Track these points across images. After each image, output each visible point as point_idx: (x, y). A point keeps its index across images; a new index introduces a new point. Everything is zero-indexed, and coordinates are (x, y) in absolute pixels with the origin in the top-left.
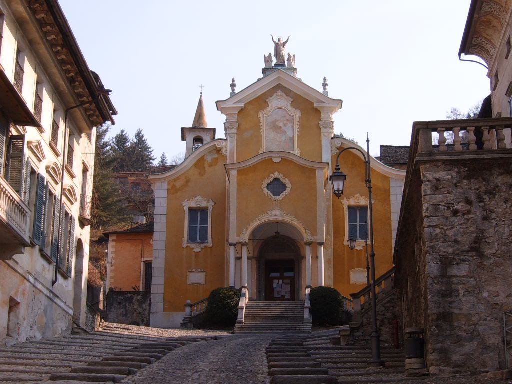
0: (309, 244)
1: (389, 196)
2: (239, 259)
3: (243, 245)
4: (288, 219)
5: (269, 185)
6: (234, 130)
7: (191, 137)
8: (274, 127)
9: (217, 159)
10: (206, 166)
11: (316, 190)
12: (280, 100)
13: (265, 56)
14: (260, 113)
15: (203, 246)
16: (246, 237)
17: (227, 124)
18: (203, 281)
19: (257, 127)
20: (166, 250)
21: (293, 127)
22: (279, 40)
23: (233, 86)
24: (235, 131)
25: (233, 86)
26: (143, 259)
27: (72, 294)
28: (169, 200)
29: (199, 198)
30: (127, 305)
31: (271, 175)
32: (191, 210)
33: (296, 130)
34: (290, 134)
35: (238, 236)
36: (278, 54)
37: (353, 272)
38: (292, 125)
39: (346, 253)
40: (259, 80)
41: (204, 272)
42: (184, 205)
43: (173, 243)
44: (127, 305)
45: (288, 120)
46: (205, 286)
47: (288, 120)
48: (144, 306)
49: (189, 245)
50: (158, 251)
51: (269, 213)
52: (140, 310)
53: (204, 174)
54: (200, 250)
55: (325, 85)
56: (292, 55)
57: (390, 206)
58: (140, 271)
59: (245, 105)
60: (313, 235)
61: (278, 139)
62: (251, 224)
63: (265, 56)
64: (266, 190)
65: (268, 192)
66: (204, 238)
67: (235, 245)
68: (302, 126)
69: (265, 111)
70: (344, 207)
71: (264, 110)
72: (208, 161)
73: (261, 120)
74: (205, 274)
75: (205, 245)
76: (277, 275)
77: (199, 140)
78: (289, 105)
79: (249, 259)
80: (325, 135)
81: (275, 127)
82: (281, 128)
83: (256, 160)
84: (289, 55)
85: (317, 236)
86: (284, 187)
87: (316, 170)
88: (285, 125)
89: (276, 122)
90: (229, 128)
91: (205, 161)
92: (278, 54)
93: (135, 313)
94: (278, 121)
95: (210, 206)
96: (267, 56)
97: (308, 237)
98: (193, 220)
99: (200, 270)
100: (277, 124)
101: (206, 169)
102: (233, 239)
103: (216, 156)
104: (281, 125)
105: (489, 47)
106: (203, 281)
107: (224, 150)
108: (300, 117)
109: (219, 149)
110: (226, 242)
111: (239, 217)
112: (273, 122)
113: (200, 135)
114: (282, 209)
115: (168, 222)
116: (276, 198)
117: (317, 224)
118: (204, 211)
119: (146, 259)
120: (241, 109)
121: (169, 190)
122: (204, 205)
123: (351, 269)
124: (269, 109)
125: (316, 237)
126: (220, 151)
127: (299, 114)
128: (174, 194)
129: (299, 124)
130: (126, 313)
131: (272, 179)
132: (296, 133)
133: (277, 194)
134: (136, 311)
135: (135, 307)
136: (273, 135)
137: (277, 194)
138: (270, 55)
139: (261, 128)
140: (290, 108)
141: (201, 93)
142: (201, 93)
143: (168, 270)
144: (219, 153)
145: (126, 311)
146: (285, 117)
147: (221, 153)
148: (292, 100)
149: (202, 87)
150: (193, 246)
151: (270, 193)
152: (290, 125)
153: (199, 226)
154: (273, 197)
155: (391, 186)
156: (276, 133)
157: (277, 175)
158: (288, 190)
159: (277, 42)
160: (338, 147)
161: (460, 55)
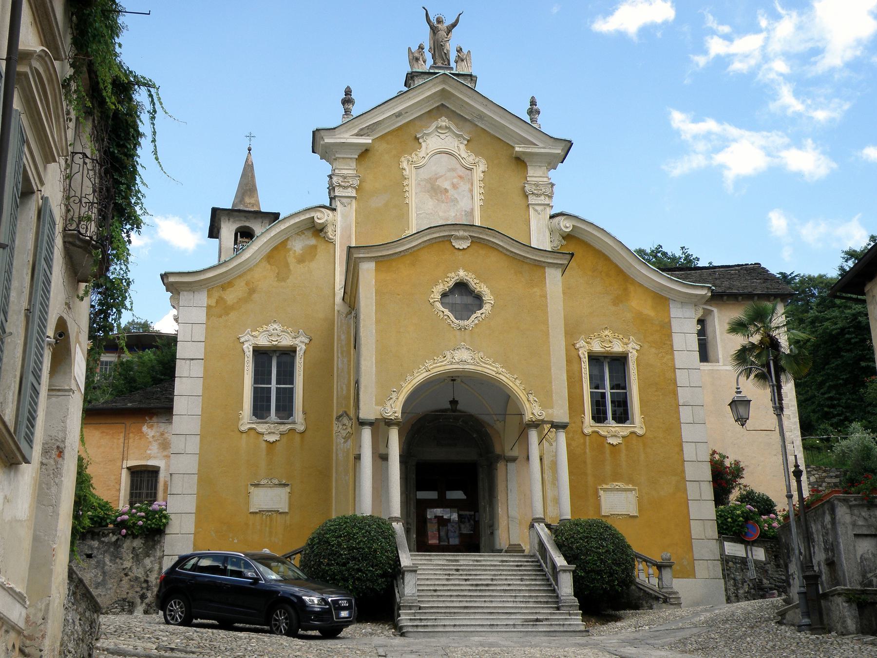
0: (536, 425)
1: (670, 336)
3: (389, 423)
4: (491, 369)
5: (444, 295)
6: (350, 190)
7: (228, 230)
8: (432, 188)
9: (315, 247)
10: (291, 260)
11: (546, 313)
12: (442, 136)
13: (409, 49)
14: (403, 159)
15: (284, 428)
16: (394, 409)
17: (335, 179)
18: (436, 497)
19: (399, 186)
20: (203, 437)
21: (471, 191)
23: (347, 101)
25: (347, 101)
26: (125, 462)
27: (25, 535)
28: (210, 330)
29: (275, 326)
30: (107, 560)
31: (449, 275)
33: (477, 197)
34: (464, 204)
35: (381, 402)
36: (438, 49)
37: (605, 490)
38: (468, 186)
39: (587, 451)
40: (401, 94)
41: (285, 485)
42: (242, 340)
44: (107, 560)
45: (461, 177)
46: (288, 517)
47: (461, 177)
48: (147, 561)
49: (254, 426)
50: (182, 438)
51: (448, 354)
52: (139, 572)
53: (288, 278)
54: (277, 437)
55: (533, 111)
56: (465, 51)
57: (673, 354)
58: (117, 487)
60: (543, 406)
61: (441, 214)
62: (409, 378)
63: (409, 49)
64: (438, 305)
65: (443, 309)
67: (371, 424)
69: (413, 155)
70: (582, 356)
71: (411, 154)
72: (295, 251)
73: (406, 173)
74: (288, 489)
75: (289, 426)
76: (432, 495)
77: (245, 234)
78: (462, 147)
80: (536, 211)
81: (434, 189)
82: (446, 190)
84: (459, 50)
85: (552, 408)
86: (478, 300)
88: (455, 186)
89: (437, 179)
90: (340, 186)
91: (289, 250)
92: (438, 49)
93: (126, 579)
96: (415, 49)
97: (532, 410)
98: (261, 375)
99: (276, 482)
100: (439, 183)
101: (291, 267)
102: (369, 410)
103: (313, 241)
104: (446, 185)
106: (436, 497)
107: (330, 230)
108: (483, 172)
109: (319, 228)
110: (335, 422)
111: (380, 362)
112: (430, 179)
113: (247, 224)
115: (206, 377)
116: (462, 323)
117: (551, 383)
118: (288, 354)
119: (132, 463)
120: (364, 149)
121: (209, 307)
122: (286, 341)
123: (600, 485)
124: (422, 153)
125: (550, 411)
126: (321, 230)
127: (482, 166)
128: (221, 316)
129: (482, 185)
130: (104, 580)
131: (451, 283)
132: (478, 203)
133: (463, 312)
134: (126, 575)
135: (127, 564)
136: (430, 204)
137: (463, 312)
138: (421, 48)
140: (464, 155)
141: (250, 150)
142: (250, 150)
143: (205, 480)
145: (104, 573)
146: (453, 170)
147: (322, 234)
149: (250, 136)
150: (261, 428)
151: (447, 312)
152: (464, 187)
153: (274, 385)
154: (454, 320)
155: (672, 316)
156: (438, 200)
157: (462, 274)
158: (487, 308)
159: (434, 20)
160: (565, 235)
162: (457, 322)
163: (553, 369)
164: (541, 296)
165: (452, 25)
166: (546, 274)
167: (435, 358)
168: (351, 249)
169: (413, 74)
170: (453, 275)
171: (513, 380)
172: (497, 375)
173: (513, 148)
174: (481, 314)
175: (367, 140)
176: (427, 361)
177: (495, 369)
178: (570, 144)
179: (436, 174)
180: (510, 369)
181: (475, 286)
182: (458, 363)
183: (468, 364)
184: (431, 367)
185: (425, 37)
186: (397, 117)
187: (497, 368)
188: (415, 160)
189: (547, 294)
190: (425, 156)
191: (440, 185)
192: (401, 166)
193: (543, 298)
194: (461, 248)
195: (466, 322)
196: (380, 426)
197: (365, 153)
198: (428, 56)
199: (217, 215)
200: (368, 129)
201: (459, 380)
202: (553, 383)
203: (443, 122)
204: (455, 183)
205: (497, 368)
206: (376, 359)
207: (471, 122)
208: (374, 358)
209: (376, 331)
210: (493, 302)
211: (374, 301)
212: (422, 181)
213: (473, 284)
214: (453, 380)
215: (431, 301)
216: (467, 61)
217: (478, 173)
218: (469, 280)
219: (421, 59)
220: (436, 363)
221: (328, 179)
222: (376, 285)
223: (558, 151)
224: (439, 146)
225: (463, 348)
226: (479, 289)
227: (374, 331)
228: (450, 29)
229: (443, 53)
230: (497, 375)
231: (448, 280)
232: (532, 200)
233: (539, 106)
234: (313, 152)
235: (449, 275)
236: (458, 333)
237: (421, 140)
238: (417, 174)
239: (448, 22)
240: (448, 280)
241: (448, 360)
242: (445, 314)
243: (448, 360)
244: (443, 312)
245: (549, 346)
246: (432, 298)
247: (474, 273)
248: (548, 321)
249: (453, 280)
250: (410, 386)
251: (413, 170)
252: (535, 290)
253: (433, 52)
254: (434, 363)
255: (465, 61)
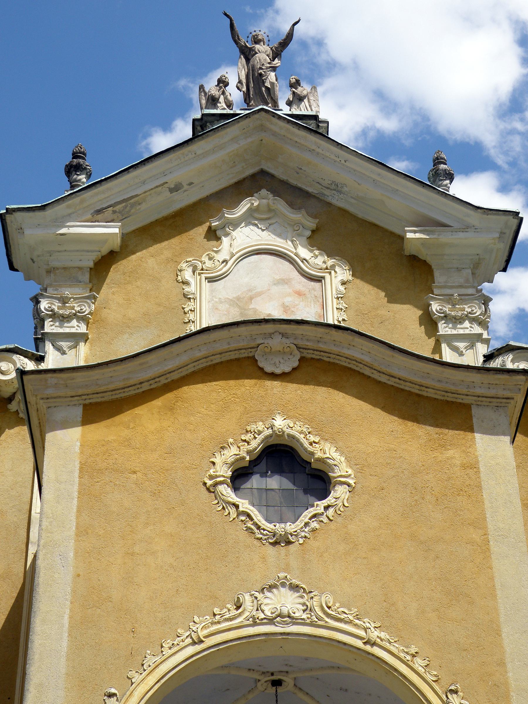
14: (184, 265)
17: (44, 305)
31: (252, 427)
45: (299, 294)
47: (299, 294)
51: (247, 601)
59: (125, 237)
62: (150, 661)
83: (184, 359)
87: (467, 407)
89: (251, 298)
94: (260, 294)
108: (343, 283)
112: (238, 298)
117: (502, 664)
131: (256, 444)
139: (191, 316)
144: (8, 410)
148: (312, 224)
154: (263, 523)
157: (279, 423)
162: (270, 526)
163: (505, 630)
164: (464, 467)
165: (280, 44)
166: (475, 420)
167: (217, 611)
168: (25, 378)
169: (205, 118)
170: (260, 426)
171: (409, 658)
172: (368, 648)
173: (402, 238)
174: (327, 508)
176: (196, 619)
177: (362, 633)
178: (516, 222)
179: (250, 290)
181: (310, 448)
182: (271, 621)
183: (294, 621)
184: (206, 632)
186: (171, 190)
187: (366, 629)
188: (209, 264)
189: (477, 462)
190: (228, 258)
191: (258, 308)
192: (179, 278)
193: (469, 471)
194: (278, 371)
195: (290, 527)
200: (114, 212)
201: (288, 680)
202: (509, 666)
204: (287, 304)
205: (366, 629)
206: (71, 617)
207: (318, 198)
208: (66, 617)
209: (76, 553)
210: (351, 482)
211: (76, 487)
212: (221, 302)
213: (306, 444)
214: (277, 683)
215: (209, 483)
216: (309, 102)
218: (297, 435)
219: (222, 99)
220: (219, 623)
221: (31, 304)
222: (82, 453)
224: (257, 240)
225: (283, 585)
226: (319, 454)
227: (72, 555)
229: (263, 89)
230: (368, 648)
231: (248, 437)
234: (12, 268)
235: (252, 427)
236: (271, 551)
237: (219, 233)
238: (212, 291)
240: (248, 437)
241: (247, 614)
242: (241, 509)
243: (247, 614)
244: (237, 506)
245: (492, 579)
246: (211, 477)
247: (309, 420)
248: (485, 519)
249: (260, 438)
250: (152, 680)
251: (206, 285)
252: (450, 453)
253: (244, 89)
254: (213, 623)
255: (306, 101)
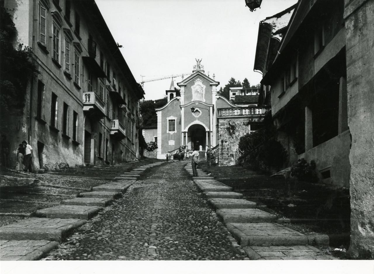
2: (185, 137)
16: (186, 130)
22: (198, 60)
24: (183, 93)
32: (169, 120)
35: (184, 129)
43: (164, 133)
66: (174, 130)
67: (184, 132)
68: (206, 91)
79: (188, 136)
95: (175, 118)
97: (207, 130)
102: (183, 130)
105: (263, 68)
114: (199, 120)
159: (197, 60)
161: (254, 70)
175: (185, 84)
180: (204, 123)
185: (196, 64)
196: (185, 133)
197: (185, 86)
198: (196, 67)
199: (167, 92)
203: (198, 79)
217: (204, 89)
223: (217, 84)
228: (200, 62)
232: (213, 92)
233: (215, 75)
239: (200, 60)
